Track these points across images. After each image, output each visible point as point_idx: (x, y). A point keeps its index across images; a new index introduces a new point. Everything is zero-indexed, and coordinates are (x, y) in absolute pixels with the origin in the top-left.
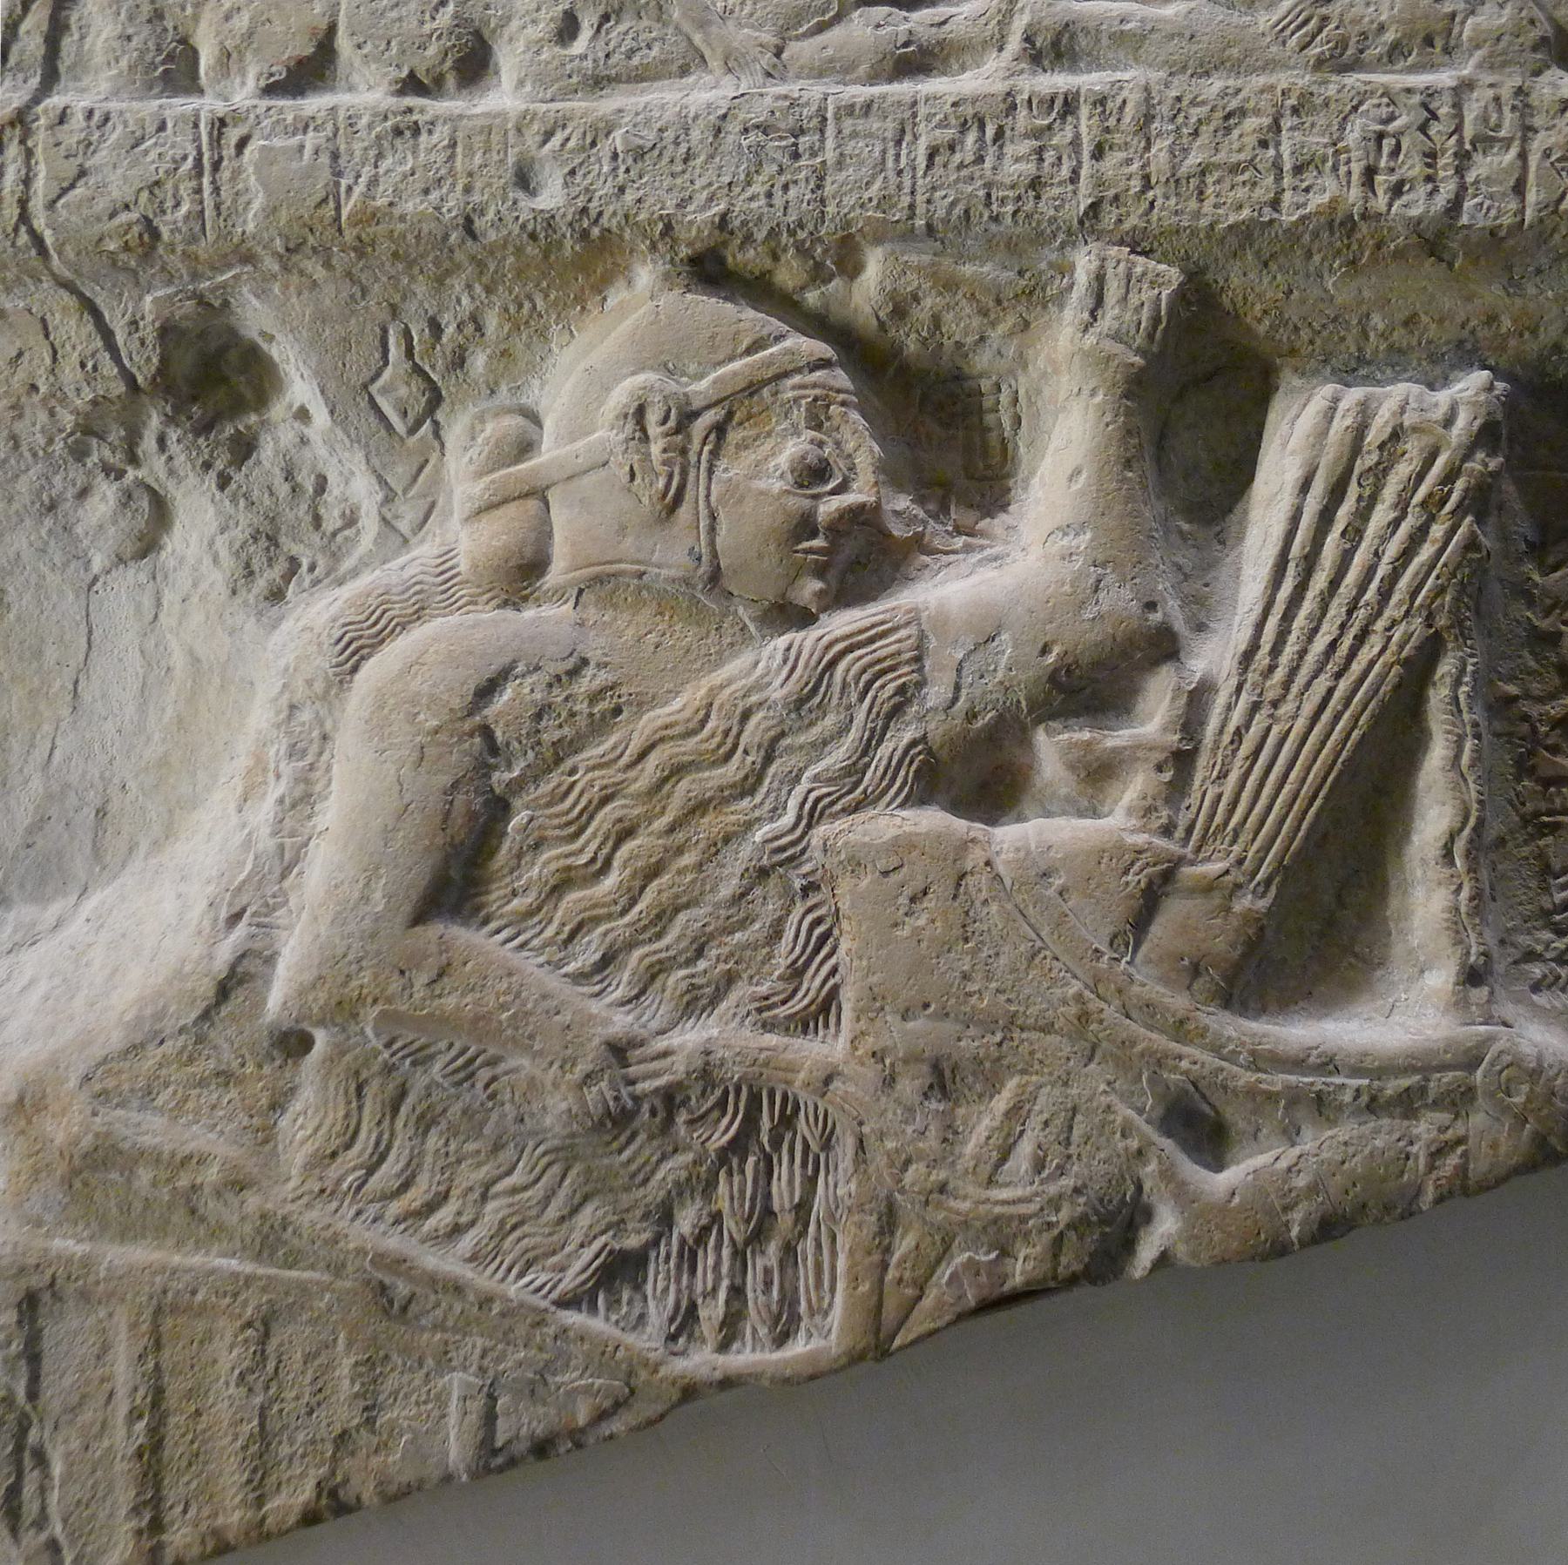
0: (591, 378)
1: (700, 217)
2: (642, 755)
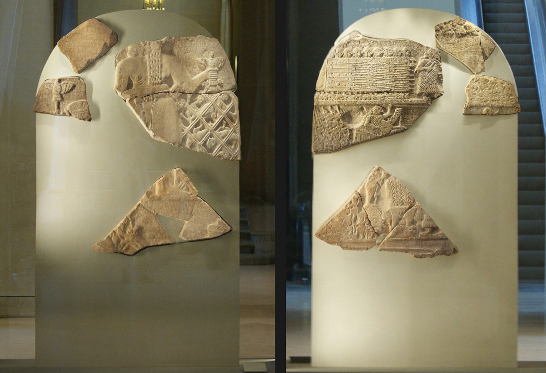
0: (374, 109)
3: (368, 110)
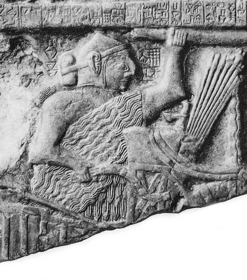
0: (85, 50)
2: (94, 116)
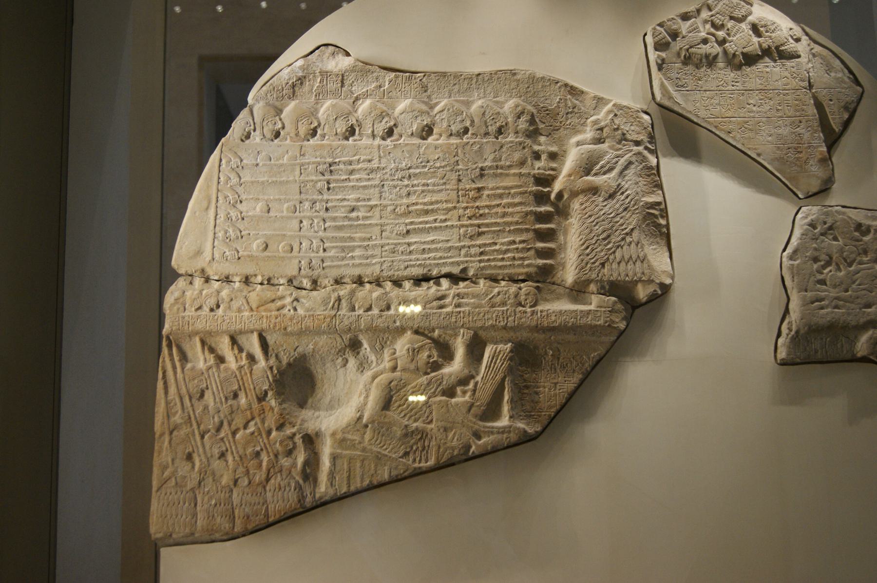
0: (402, 345)
1: (416, 326)
3: (379, 351)
